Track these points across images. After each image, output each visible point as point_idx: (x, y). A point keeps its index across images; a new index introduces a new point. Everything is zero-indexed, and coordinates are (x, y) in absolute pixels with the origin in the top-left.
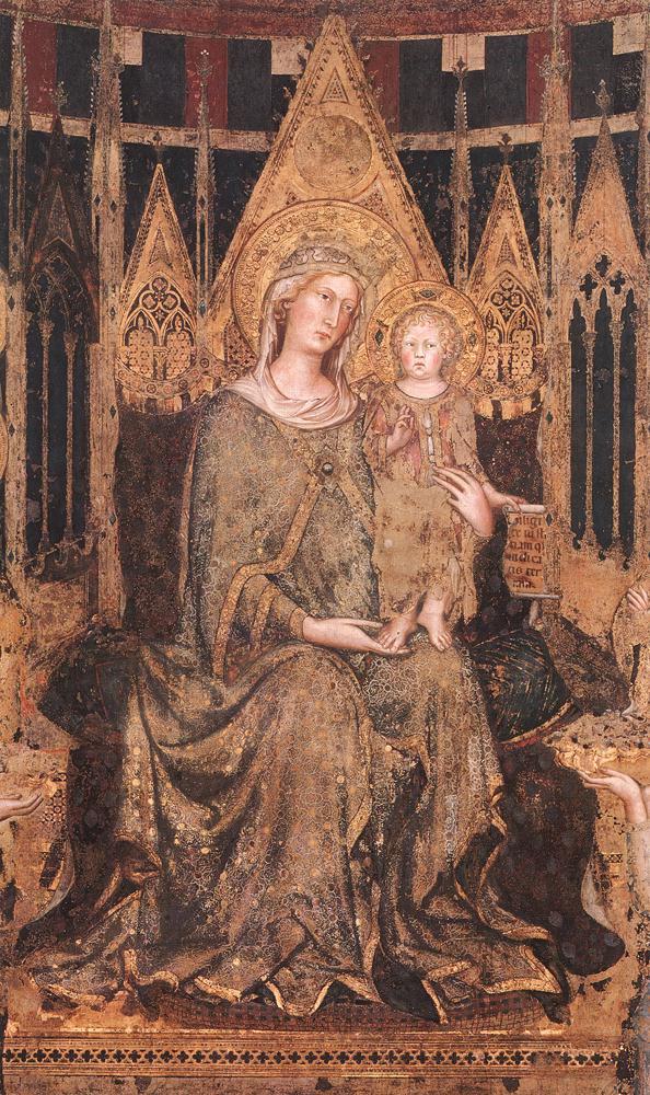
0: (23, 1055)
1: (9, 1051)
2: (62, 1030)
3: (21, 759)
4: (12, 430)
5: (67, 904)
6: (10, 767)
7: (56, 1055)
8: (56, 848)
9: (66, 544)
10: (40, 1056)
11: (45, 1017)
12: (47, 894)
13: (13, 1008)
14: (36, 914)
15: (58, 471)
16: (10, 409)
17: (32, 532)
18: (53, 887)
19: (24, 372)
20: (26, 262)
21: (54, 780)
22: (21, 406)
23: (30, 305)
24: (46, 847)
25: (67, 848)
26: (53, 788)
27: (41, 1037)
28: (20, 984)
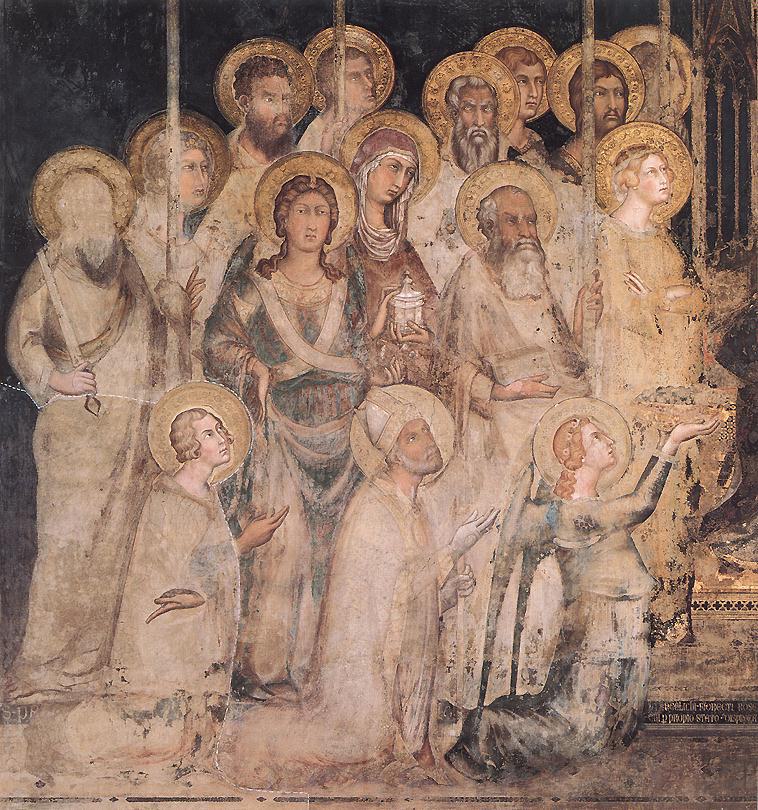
0: (706, 606)
1: (695, 602)
2: (733, 587)
3: (704, 395)
4: (696, 162)
5: (736, 498)
6: (696, 401)
7: (728, 605)
8: (729, 458)
9: (734, 243)
10: (717, 606)
11: (721, 578)
12: (723, 490)
13: (698, 572)
14: (715, 505)
15: (729, 191)
16: (694, 147)
17: (711, 234)
18: (726, 486)
19: (704, 120)
20: (705, 42)
21: (728, 409)
22: (702, 145)
23: (708, 73)
24: (722, 458)
25: (736, 459)
26: (727, 415)
27: (718, 593)
28: (703, 554)
